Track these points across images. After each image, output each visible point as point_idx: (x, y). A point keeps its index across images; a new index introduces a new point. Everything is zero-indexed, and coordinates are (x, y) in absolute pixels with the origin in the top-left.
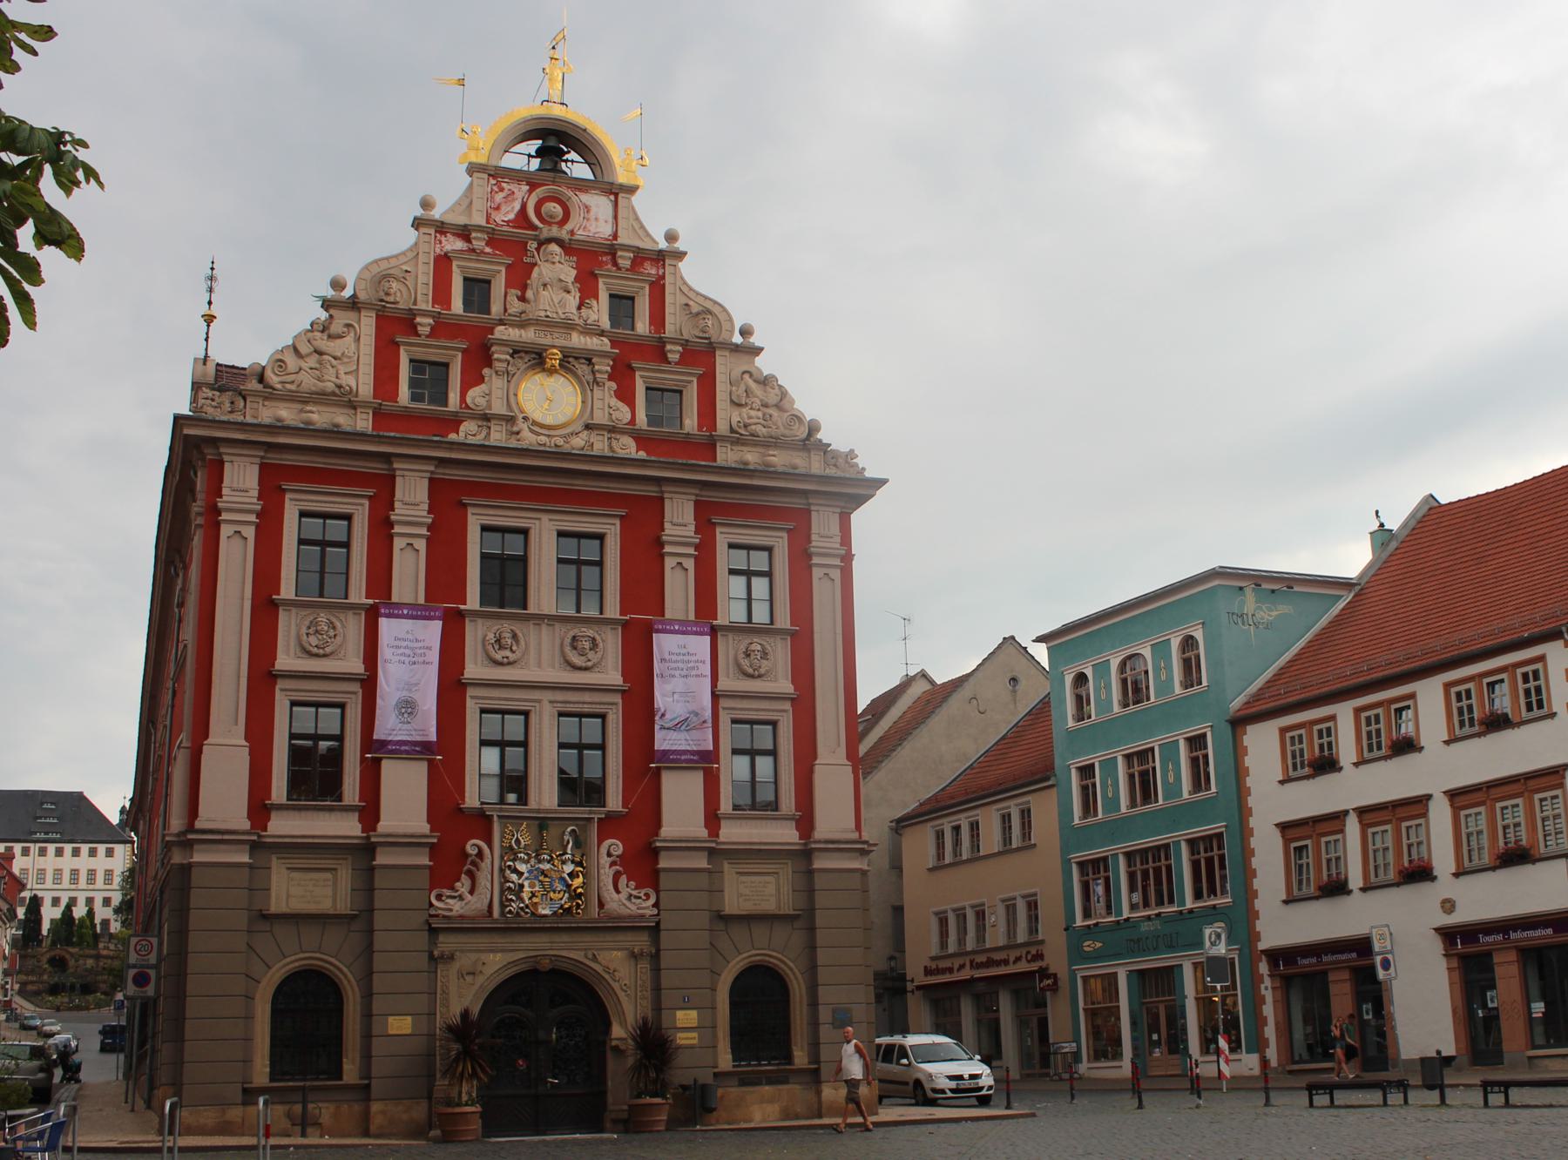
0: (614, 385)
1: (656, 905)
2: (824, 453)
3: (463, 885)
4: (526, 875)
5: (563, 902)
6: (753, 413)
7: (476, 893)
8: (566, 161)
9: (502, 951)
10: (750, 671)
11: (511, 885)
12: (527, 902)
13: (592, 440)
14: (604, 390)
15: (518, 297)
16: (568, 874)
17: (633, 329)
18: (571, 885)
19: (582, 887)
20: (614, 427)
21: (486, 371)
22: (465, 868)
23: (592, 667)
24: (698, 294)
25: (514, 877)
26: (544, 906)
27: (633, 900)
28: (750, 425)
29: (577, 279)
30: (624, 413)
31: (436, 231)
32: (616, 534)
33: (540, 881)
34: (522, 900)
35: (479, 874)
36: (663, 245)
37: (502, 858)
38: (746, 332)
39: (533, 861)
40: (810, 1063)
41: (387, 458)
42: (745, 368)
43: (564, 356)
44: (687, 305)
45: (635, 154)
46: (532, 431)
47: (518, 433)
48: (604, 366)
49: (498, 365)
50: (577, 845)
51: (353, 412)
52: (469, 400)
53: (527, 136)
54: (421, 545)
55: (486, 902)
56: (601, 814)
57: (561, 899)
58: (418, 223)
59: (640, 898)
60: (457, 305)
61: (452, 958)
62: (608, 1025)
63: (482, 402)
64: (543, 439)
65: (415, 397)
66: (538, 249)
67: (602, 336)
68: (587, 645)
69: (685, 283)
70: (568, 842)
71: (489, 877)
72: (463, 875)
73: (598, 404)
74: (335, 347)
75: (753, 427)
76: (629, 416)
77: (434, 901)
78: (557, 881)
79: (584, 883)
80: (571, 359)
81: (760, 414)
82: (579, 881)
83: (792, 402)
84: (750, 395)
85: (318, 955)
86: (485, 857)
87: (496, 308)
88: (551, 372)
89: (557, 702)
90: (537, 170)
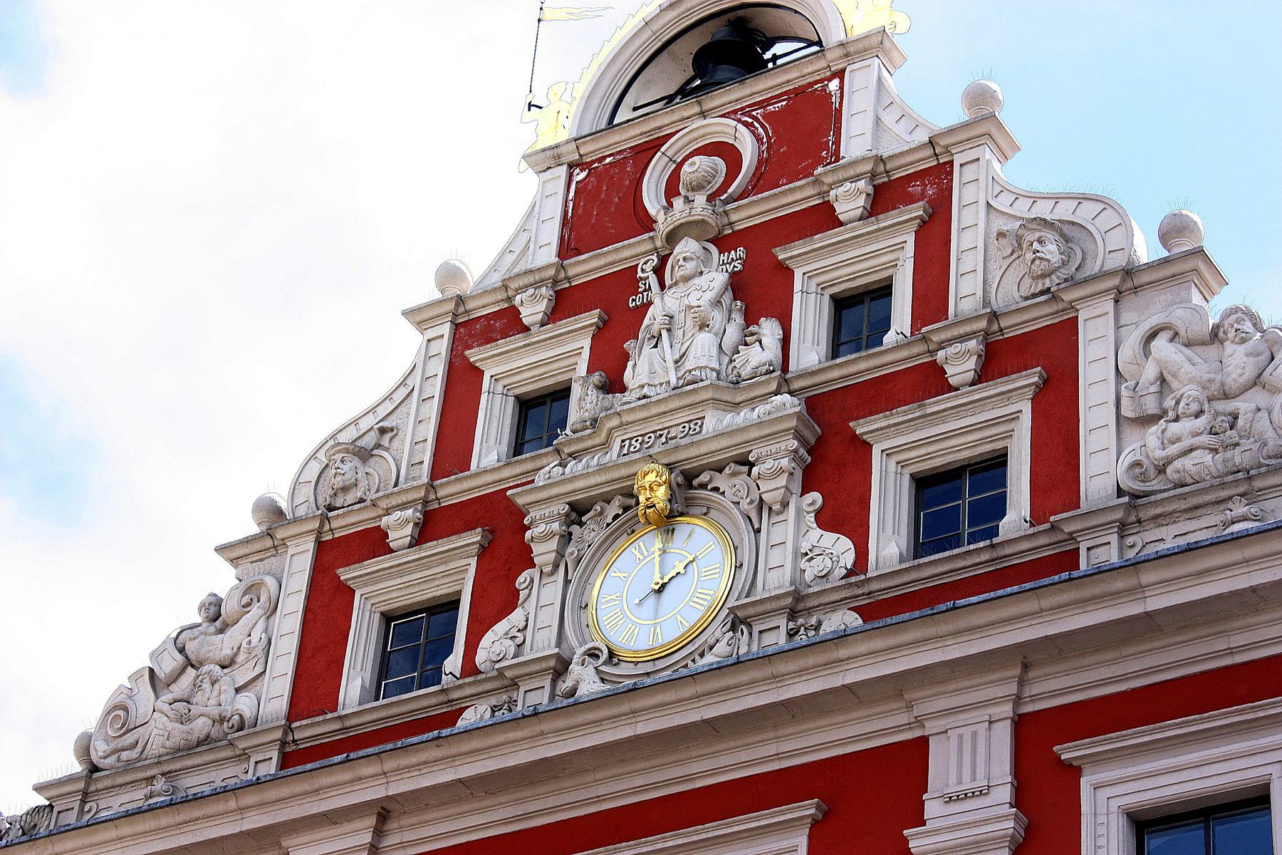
49: (543, 552)
75: (1177, 464)
76: (849, 559)
80: (704, 478)
88: (667, 522)
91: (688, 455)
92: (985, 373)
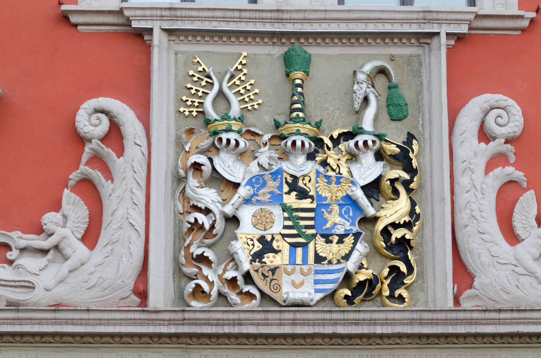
3: (65, 217)
4: (243, 191)
7: (104, 237)
11: (201, 218)
12: (246, 266)
16: (363, 188)
18: (375, 219)
19: (408, 225)
22: (74, 176)
26: (297, 277)
33: (285, 208)
34: (232, 258)
37: (180, 145)
57: (347, 257)
70: (366, 100)
72: (66, 190)
78: (336, 208)
79: (412, 212)
86: (128, 143)
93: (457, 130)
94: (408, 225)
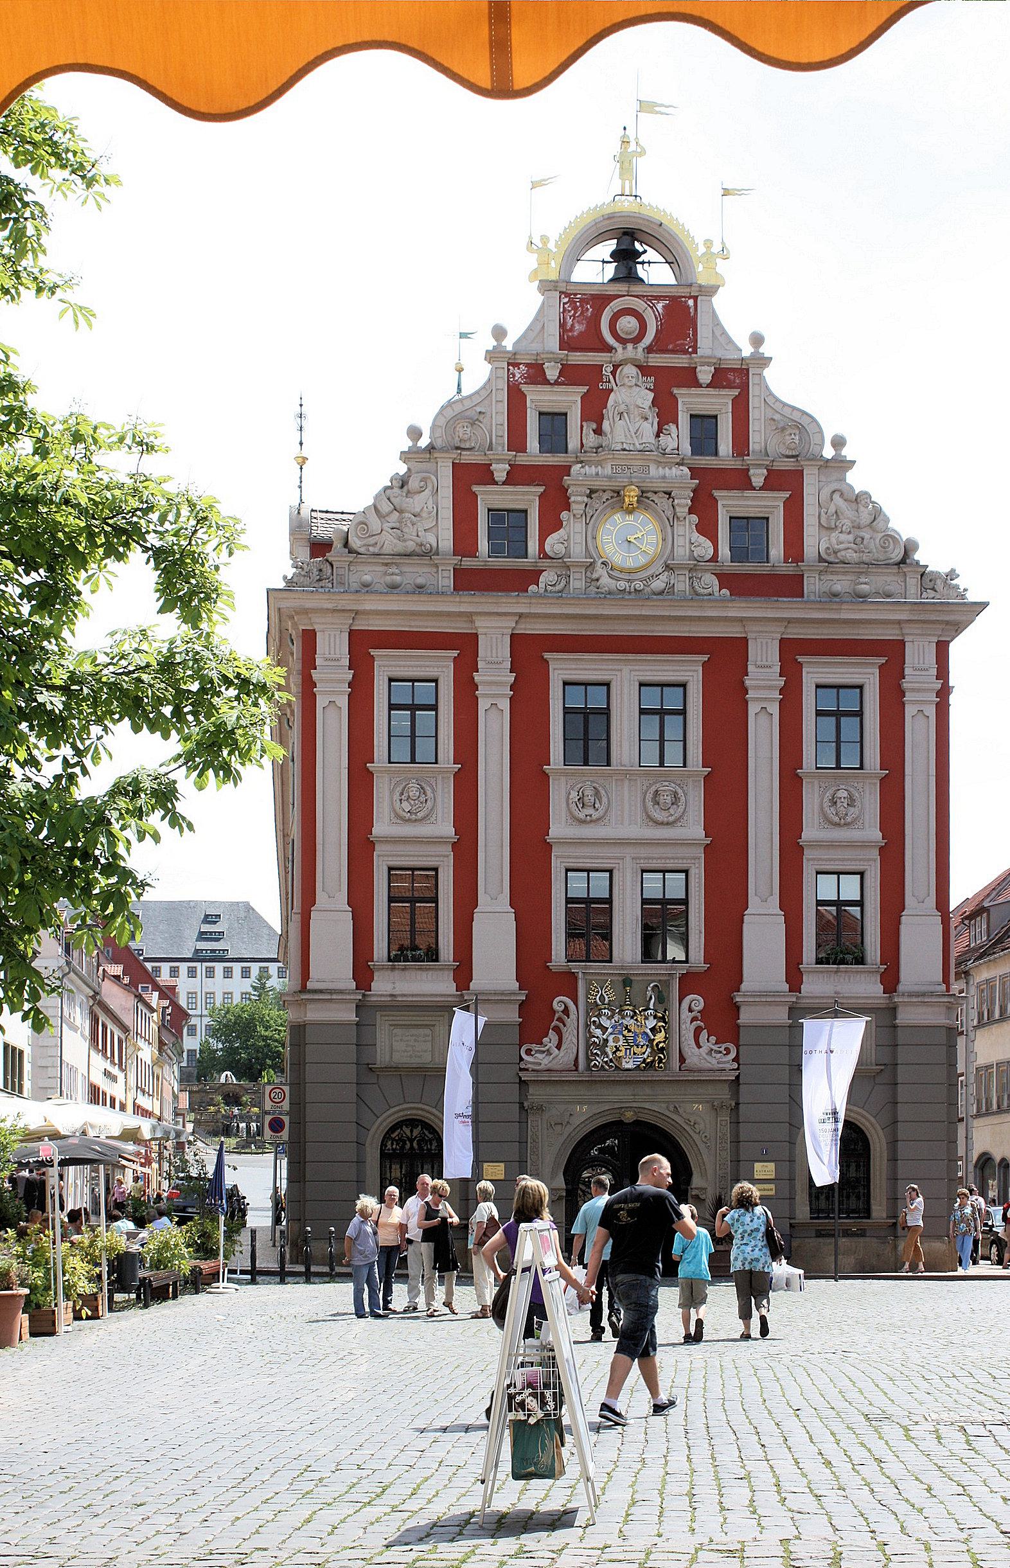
0: (694, 518)
1: (736, 1059)
2: (922, 575)
4: (610, 1030)
5: (645, 1056)
6: (843, 537)
7: (563, 1047)
8: (643, 263)
9: (589, 1103)
10: (836, 819)
11: (596, 1040)
13: (672, 582)
14: (685, 525)
15: (594, 431)
17: (716, 454)
19: (664, 1042)
20: (695, 565)
21: (564, 515)
23: (674, 822)
24: (785, 404)
25: (598, 1032)
27: (714, 1055)
28: (840, 551)
29: (654, 403)
30: (705, 547)
31: (509, 364)
32: (698, 681)
33: (624, 1036)
35: (564, 1030)
36: (747, 351)
37: (588, 1014)
38: (839, 443)
39: (616, 1017)
40: (888, 1217)
41: (470, 616)
42: (834, 486)
43: (643, 492)
44: (773, 419)
45: (716, 248)
46: (610, 576)
47: (597, 580)
48: (684, 501)
49: (577, 508)
50: (661, 1000)
51: (435, 570)
52: (547, 548)
53: (600, 238)
54: (505, 705)
55: (573, 1057)
56: (683, 969)
58: (491, 356)
59: (720, 1052)
60: (533, 443)
61: (540, 1109)
62: (690, 1175)
63: (560, 549)
64: (622, 585)
65: (494, 551)
66: (614, 373)
67: (682, 464)
68: (669, 800)
69: (771, 394)
70: (651, 998)
71: (575, 1032)
73: (679, 541)
74: (417, 503)
75: (843, 553)
77: (524, 1056)
79: (665, 1037)
80: (649, 495)
81: (851, 537)
82: (660, 1037)
83: (887, 520)
84: (841, 517)
85: (420, 1106)
87: (573, 443)
88: (630, 511)
89: (640, 858)
90: (611, 280)
91: (647, 485)
92: (768, 486)
93: (682, 1008)
94: (664, 1042)
